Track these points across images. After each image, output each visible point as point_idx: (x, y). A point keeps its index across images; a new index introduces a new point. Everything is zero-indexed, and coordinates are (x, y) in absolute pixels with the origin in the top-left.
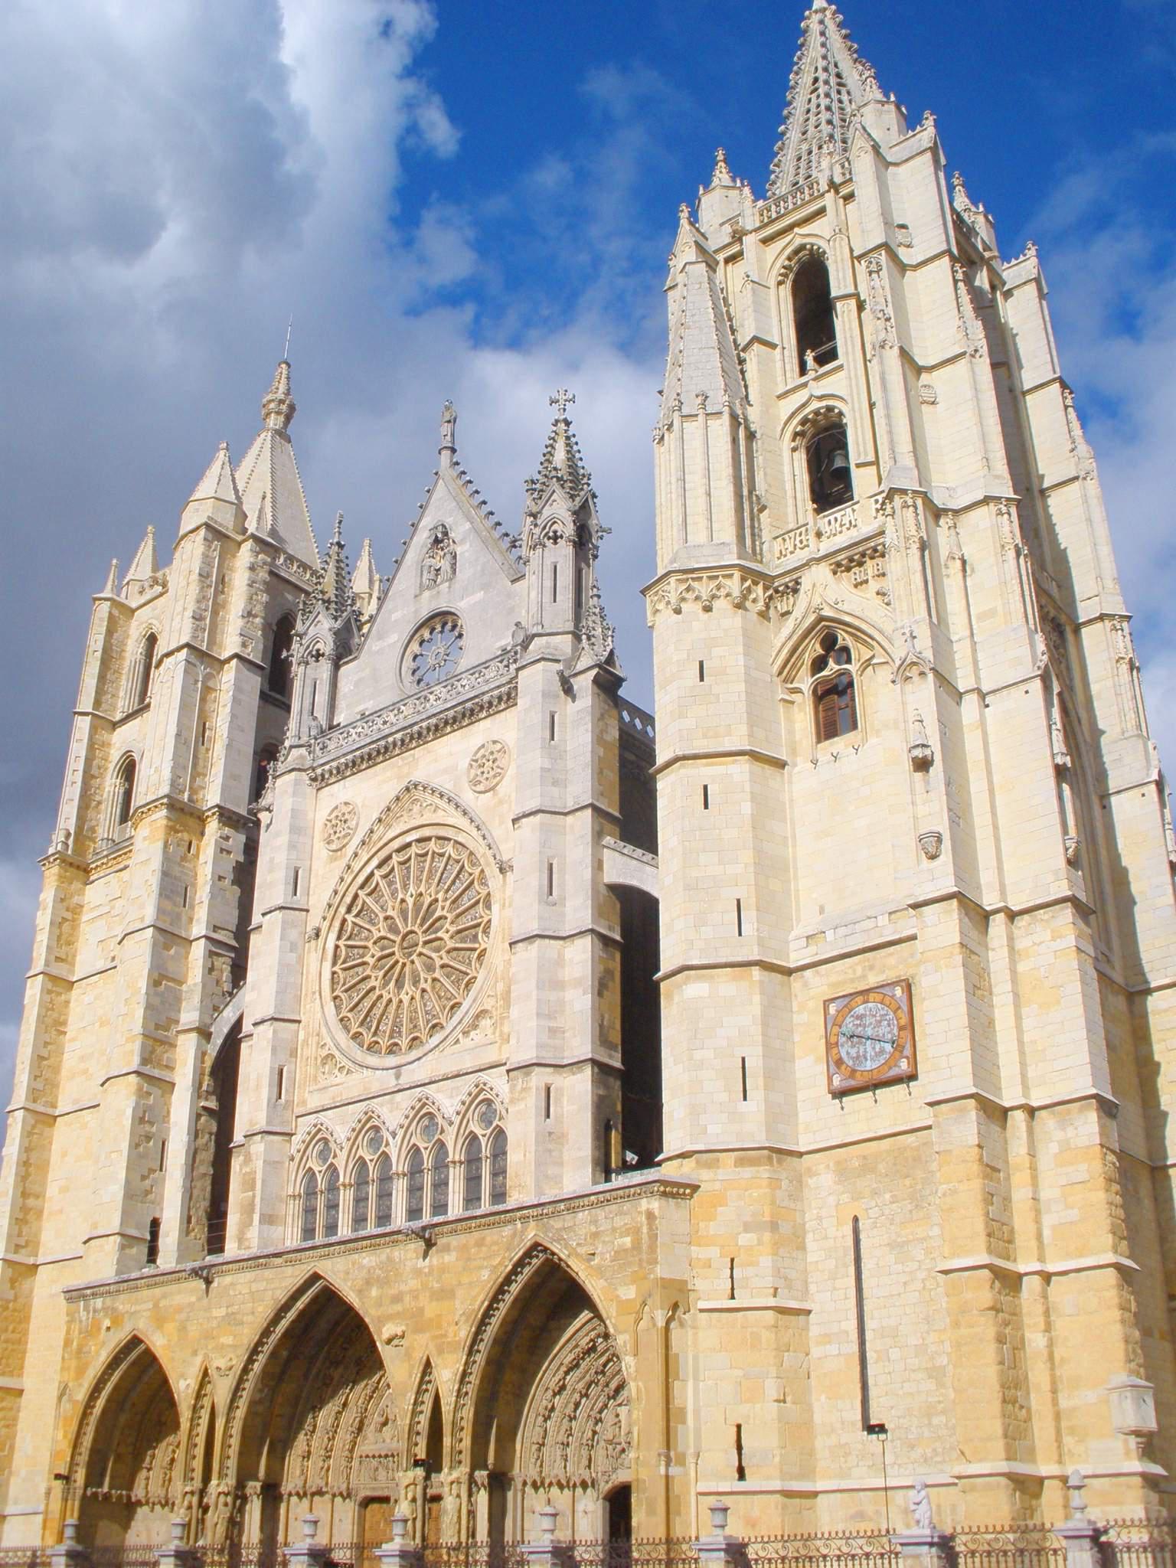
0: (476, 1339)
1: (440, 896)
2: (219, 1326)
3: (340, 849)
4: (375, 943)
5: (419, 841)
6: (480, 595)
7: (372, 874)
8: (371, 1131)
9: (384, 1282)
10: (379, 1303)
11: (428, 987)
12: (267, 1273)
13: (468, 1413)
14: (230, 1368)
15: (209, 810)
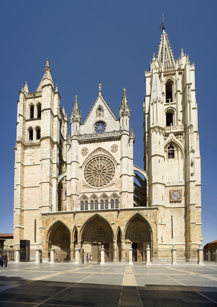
0: (127, 225)
1: (105, 166)
2: (77, 220)
3: (85, 155)
4: (93, 171)
5: (100, 157)
6: (109, 121)
7: (91, 160)
8: (94, 197)
9: (111, 216)
10: (110, 219)
11: (103, 178)
12: (87, 213)
13: (125, 234)
14: (81, 226)
15: (55, 142)
